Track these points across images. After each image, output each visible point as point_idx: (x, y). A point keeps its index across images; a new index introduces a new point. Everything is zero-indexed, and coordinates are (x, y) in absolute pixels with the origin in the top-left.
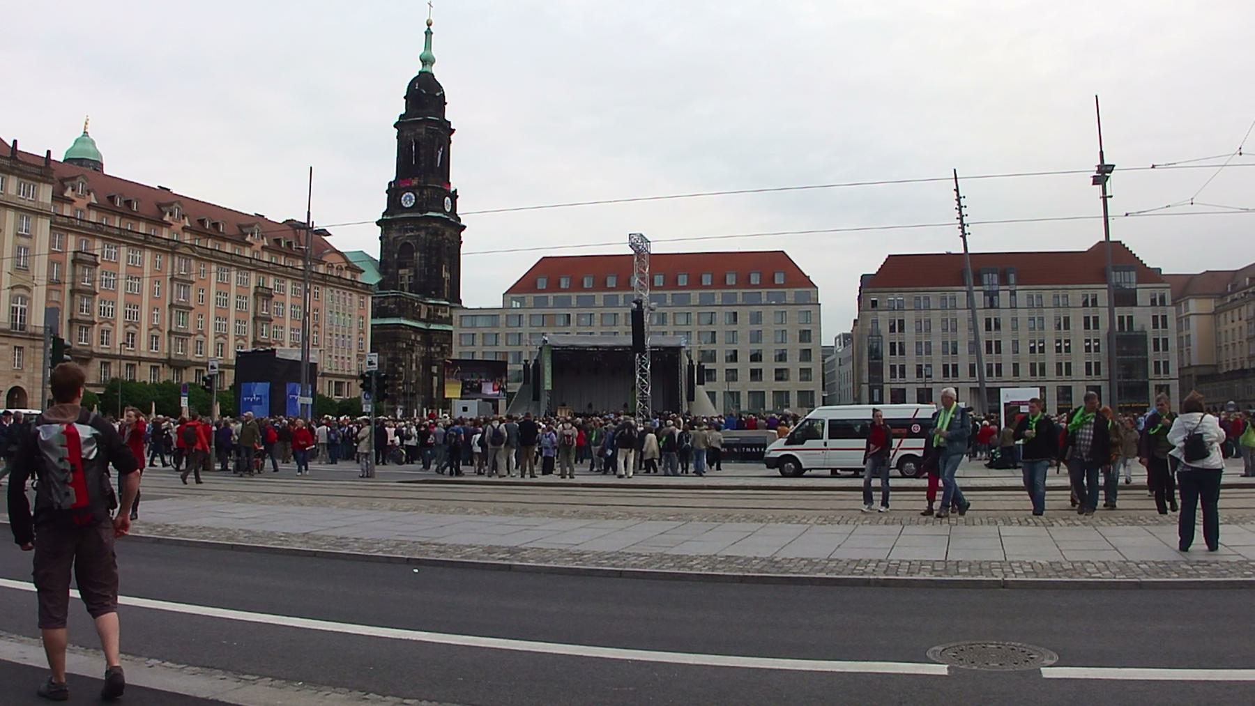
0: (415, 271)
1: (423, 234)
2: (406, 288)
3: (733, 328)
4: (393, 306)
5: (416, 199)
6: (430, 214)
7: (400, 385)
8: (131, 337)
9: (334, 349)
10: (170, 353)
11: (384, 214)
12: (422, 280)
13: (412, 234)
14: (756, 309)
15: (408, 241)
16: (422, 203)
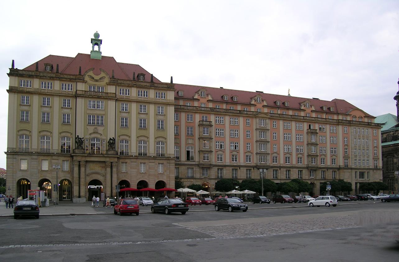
8: (234, 158)
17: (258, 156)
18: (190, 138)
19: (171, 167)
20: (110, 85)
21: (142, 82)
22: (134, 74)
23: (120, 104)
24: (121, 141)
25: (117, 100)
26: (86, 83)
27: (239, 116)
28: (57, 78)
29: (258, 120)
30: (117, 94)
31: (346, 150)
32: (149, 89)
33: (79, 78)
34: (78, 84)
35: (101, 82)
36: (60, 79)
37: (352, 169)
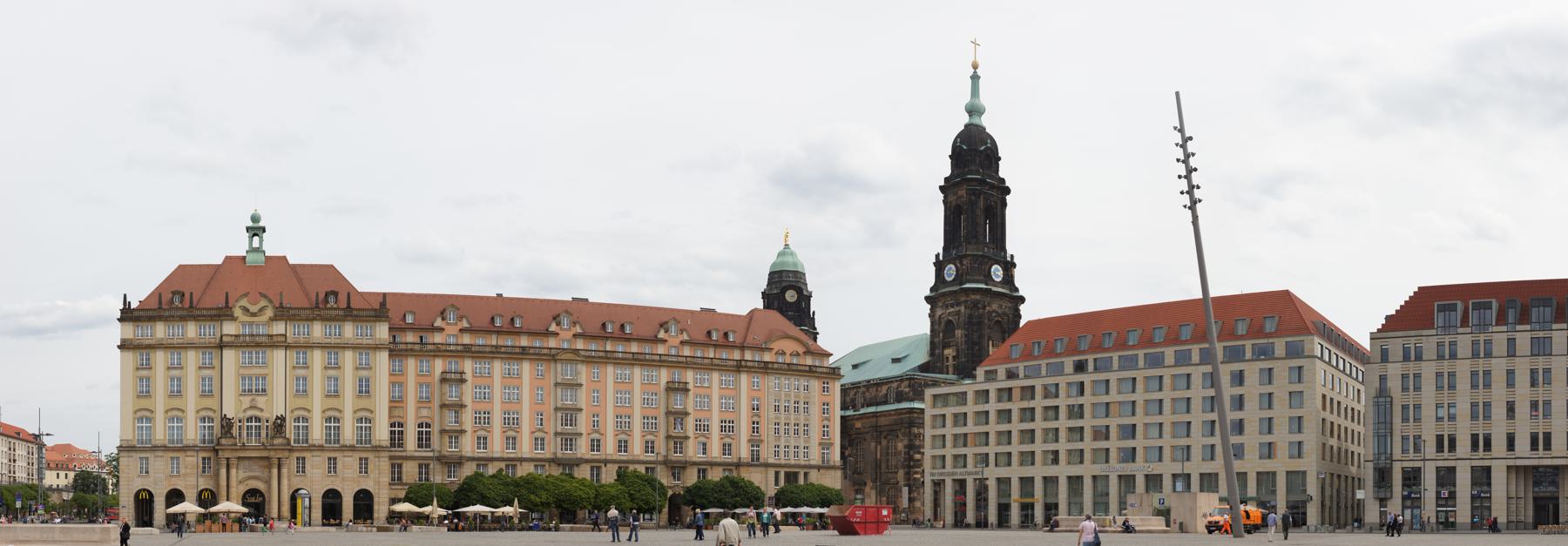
0: (958, 351)
1: (962, 309)
2: (951, 369)
3: (1269, 389)
4: (907, 390)
5: (957, 271)
6: (967, 286)
7: (917, 473)
8: (512, 441)
9: (783, 439)
10: (555, 454)
11: (932, 290)
12: (963, 360)
13: (952, 310)
14: (1237, 367)
15: (950, 318)
16: (962, 275)
17: (559, 439)
18: (425, 405)
19: (381, 463)
20: (276, 320)
21: (331, 309)
22: (317, 295)
23: (292, 354)
24: (326, 420)
25: (286, 347)
26: (236, 320)
27: (522, 359)
28: (190, 316)
29: (559, 366)
30: (288, 335)
31: (756, 425)
32: (344, 321)
33: (223, 313)
34: (225, 323)
35: (261, 315)
36: (196, 318)
37: (767, 465)
